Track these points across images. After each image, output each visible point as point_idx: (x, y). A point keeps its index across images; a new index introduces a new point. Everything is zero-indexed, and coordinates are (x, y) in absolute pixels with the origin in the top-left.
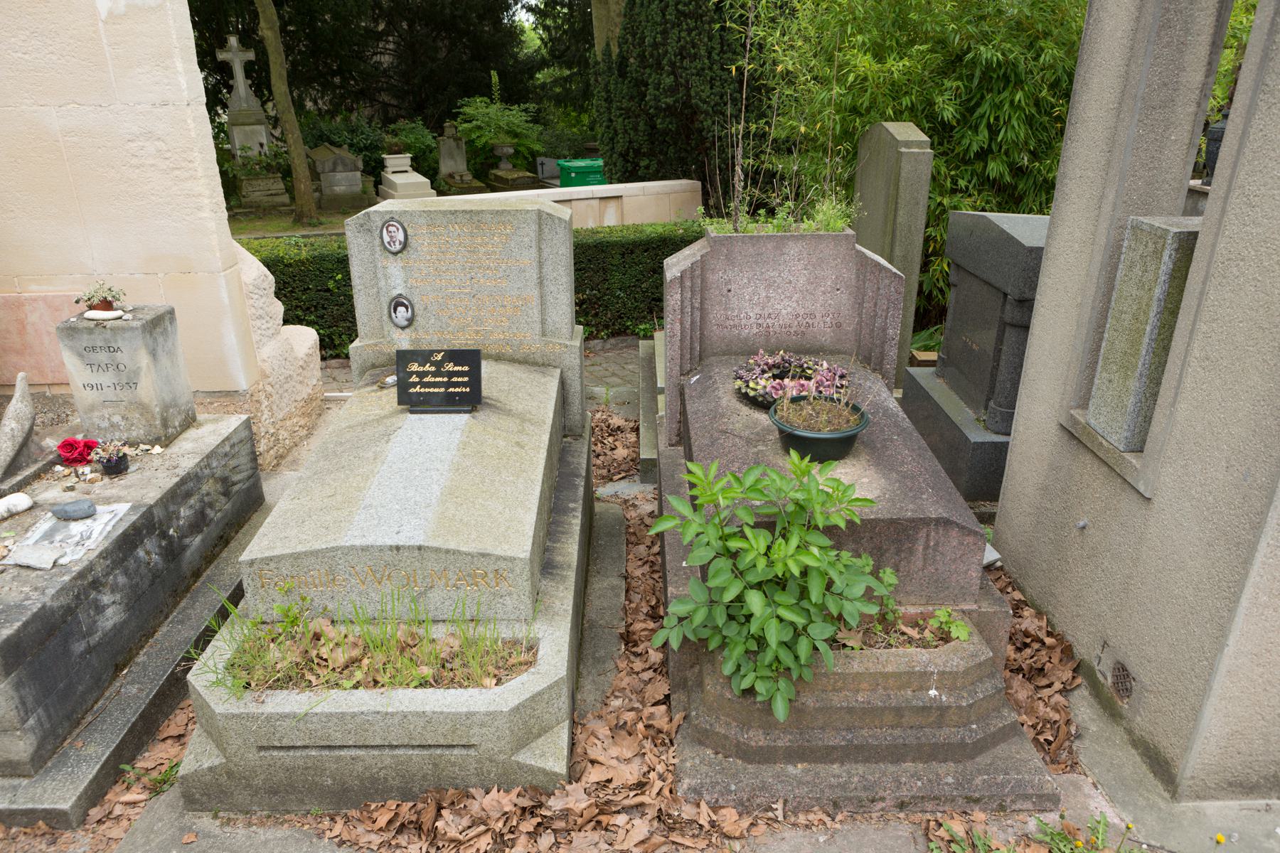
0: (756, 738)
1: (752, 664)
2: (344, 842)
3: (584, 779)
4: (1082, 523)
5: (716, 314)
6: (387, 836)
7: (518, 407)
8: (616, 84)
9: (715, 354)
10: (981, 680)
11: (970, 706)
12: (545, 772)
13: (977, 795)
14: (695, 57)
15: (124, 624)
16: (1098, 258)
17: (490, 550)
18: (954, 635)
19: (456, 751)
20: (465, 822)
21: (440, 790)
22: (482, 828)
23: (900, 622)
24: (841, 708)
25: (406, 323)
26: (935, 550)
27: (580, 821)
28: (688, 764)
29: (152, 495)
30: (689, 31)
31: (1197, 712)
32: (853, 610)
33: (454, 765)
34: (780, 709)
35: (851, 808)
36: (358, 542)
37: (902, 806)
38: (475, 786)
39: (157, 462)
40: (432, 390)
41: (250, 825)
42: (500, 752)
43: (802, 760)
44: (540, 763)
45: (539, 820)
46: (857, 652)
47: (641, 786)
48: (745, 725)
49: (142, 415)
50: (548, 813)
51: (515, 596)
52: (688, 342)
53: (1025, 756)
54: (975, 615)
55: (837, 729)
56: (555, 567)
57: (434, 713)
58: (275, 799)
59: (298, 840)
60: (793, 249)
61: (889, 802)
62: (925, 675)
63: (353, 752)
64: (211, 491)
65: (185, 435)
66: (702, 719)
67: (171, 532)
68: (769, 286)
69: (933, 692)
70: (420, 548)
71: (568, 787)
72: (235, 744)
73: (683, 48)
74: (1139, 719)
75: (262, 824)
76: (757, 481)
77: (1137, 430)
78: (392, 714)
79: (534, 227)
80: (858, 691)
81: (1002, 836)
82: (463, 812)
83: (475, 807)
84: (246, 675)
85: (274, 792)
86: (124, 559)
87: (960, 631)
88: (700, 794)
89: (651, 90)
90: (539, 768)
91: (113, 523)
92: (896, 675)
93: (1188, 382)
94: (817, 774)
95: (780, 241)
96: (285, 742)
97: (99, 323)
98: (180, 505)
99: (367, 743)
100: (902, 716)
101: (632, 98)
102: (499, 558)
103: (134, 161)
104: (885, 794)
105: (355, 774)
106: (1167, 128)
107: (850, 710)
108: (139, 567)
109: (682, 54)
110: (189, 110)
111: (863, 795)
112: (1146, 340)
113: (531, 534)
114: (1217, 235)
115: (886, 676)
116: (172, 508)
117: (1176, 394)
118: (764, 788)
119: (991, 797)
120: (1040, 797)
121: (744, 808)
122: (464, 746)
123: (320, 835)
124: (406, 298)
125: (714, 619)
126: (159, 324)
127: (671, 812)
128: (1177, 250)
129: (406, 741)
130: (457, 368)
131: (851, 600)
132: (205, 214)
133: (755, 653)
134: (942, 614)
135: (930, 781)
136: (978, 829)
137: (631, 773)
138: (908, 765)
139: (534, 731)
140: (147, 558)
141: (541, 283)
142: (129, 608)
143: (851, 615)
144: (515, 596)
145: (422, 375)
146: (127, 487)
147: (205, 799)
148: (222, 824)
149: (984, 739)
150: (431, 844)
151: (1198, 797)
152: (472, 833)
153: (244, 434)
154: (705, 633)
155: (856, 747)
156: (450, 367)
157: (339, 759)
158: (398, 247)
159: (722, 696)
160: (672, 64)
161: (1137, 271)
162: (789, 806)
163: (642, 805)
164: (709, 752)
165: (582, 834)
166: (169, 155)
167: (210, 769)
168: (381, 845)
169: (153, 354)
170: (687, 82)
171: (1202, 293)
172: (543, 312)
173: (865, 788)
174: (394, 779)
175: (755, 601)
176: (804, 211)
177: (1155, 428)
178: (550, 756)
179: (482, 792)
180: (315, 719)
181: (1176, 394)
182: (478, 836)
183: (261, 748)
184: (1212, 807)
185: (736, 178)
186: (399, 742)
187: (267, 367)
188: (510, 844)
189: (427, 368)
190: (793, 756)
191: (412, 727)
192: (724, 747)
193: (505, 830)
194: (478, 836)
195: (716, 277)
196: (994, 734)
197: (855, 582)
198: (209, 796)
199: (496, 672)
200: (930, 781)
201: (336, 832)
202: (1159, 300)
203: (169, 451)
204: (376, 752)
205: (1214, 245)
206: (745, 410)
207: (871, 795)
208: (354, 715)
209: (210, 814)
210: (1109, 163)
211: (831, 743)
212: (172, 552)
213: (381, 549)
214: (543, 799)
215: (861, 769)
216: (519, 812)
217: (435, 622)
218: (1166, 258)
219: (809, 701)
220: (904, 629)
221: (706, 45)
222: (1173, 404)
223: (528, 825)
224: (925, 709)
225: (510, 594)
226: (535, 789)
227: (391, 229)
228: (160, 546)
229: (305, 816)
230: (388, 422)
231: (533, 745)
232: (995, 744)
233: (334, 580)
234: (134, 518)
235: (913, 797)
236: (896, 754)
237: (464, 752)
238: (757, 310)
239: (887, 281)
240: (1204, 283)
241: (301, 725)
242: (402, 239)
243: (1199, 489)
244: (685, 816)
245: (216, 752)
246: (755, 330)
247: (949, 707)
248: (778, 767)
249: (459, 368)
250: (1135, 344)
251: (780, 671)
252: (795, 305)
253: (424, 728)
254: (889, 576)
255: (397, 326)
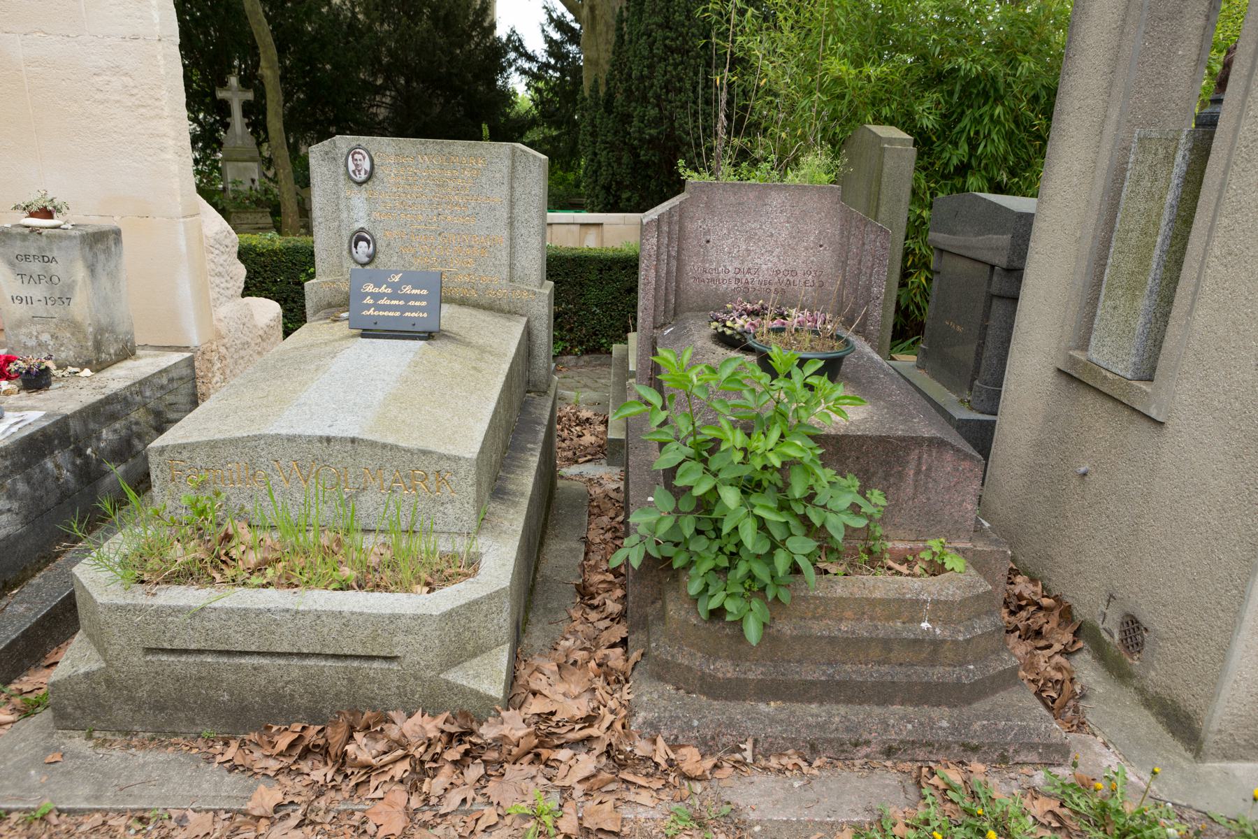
0: (724, 669)
1: (721, 583)
2: (236, 767)
3: (524, 710)
4: (1082, 470)
5: (693, 266)
6: (287, 761)
7: (475, 340)
8: (602, 118)
9: (690, 310)
10: (978, 616)
11: (968, 641)
12: (477, 695)
13: (975, 742)
14: (680, 90)
15: (19, 538)
16: (1100, 183)
17: (432, 448)
18: (948, 566)
19: (376, 664)
20: (381, 746)
21: (355, 712)
22: (400, 752)
23: (887, 556)
24: (822, 637)
25: (367, 259)
26: (927, 476)
27: (515, 751)
28: (645, 699)
29: (70, 407)
30: (676, 66)
31: (1224, 651)
32: (836, 525)
33: (372, 681)
34: (752, 632)
35: (831, 753)
36: (284, 432)
37: (889, 752)
38: (395, 709)
39: (82, 383)
40: (386, 313)
41: (128, 746)
42: (427, 667)
43: (776, 696)
44: (473, 684)
45: (468, 746)
46: (840, 578)
47: (589, 720)
48: (712, 655)
49: (73, 334)
50: (479, 741)
51: (458, 504)
52: (662, 292)
53: (1026, 704)
54: (970, 554)
55: (815, 663)
56: (505, 493)
57: (352, 613)
58: (162, 717)
59: (182, 764)
60: (776, 199)
61: (874, 748)
62: (917, 603)
63: (256, 661)
64: (142, 421)
65: (119, 365)
66: (662, 648)
67: (89, 451)
68: (750, 238)
69: (925, 625)
70: (353, 440)
71: (504, 714)
72: (118, 643)
73: (669, 82)
74: (1153, 673)
75: (143, 746)
76: (733, 374)
77: (1146, 355)
78: (304, 613)
79: (508, 162)
80: (841, 620)
81: (1005, 788)
82: (379, 736)
83: (394, 732)
84: (141, 571)
85: (159, 707)
86: (28, 465)
87: (954, 562)
88: (657, 730)
89: (636, 122)
90: (472, 690)
91: (20, 425)
92: (885, 602)
93: (1207, 285)
94: (793, 713)
95: (764, 190)
96: (177, 644)
97: (33, 230)
98: (102, 425)
99: (272, 649)
100: (891, 650)
101: (615, 133)
102: (442, 457)
103: (99, 96)
104: (870, 737)
105: (256, 688)
106: (1174, 42)
107: (832, 640)
108: (45, 479)
109: (667, 87)
110: (160, 46)
111: (845, 736)
112: (1157, 252)
113: (481, 439)
114: (1239, 117)
115: (872, 602)
116: (92, 426)
117: (1193, 301)
118: (731, 724)
119: (991, 745)
120: (1047, 746)
121: (707, 747)
122: (385, 658)
123: (209, 760)
124: (367, 233)
125: (681, 530)
126: (101, 242)
127: (621, 747)
128: (1191, 150)
129: (318, 649)
130: (415, 292)
131: (836, 513)
132: (169, 156)
133: (727, 570)
134: (935, 544)
135: (921, 724)
136: (977, 778)
137: (581, 708)
138: (897, 708)
139: (469, 647)
140: (56, 472)
141: (511, 224)
142: (27, 521)
143: (837, 528)
144: (458, 504)
145: (376, 296)
146: (44, 400)
147: (78, 713)
148: (96, 746)
149: (982, 681)
150: (338, 771)
151: (1227, 757)
152: (387, 758)
153: (185, 372)
154: (669, 550)
155: (838, 683)
156: (408, 290)
157: (239, 668)
158: (363, 176)
159: (686, 621)
160: (658, 97)
161: (1146, 183)
162: (760, 748)
163: (589, 739)
164: (669, 687)
165: (518, 766)
166: (135, 91)
167: (87, 675)
168: (278, 772)
169: (92, 269)
170: (671, 114)
171: (1222, 185)
172: (512, 255)
173: (848, 730)
174: (301, 697)
175: (730, 497)
176: (786, 162)
177: (1168, 344)
178: (486, 676)
179: (404, 715)
180: (213, 616)
181: (1193, 301)
182: (394, 762)
183: (149, 651)
184: (1240, 768)
185: (719, 125)
186: (311, 650)
187: (223, 328)
188: (431, 773)
189: (383, 289)
190: (768, 691)
191: (326, 630)
192: (686, 681)
193: (427, 757)
194: (394, 762)
195: (694, 226)
196: (993, 677)
197: (841, 501)
198: (83, 709)
199: (430, 580)
200: (921, 724)
201: (228, 756)
202: (1172, 206)
203: (98, 376)
204: (282, 662)
205: (1236, 130)
206: (721, 350)
207: (853, 737)
208: (259, 613)
209: (83, 734)
210: (1111, 84)
211: (809, 678)
212: (89, 475)
213: (310, 440)
214: (475, 726)
215: (843, 709)
216: (444, 739)
217: (366, 531)
218: (1179, 159)
219: (786, 628)
220: (891, 563)
221: (691, 79)
222: (1190, 313)
223: (455, 753)
224: (916, 642)
225: (452, 501)
226: (465, 715)
227: (357, 156)
228: (74, 463)
229: (195, 739)
230: (336, 344)
231: (467, 664)
232: (994, 691)
233: (254, 475)
234: (45, 424)
235: (902, 742)
236: (882, 694)
237: (385, 665)
238: (737, 264)
239: (872, 236)
240: (1225, 173)
241: (197, 623)
242: (368, 168)
243: (1223, 398)
244: (638, 752)
245: (97, 656)
246: (733, 286)
247: (943, 641)
248: (748, 705)
249: (418, 292)
250: (1143, 261)
251: (754, 588)
252: (776, 260)
253: (340, 632)
254: (877, 496)
255: (356, 262)
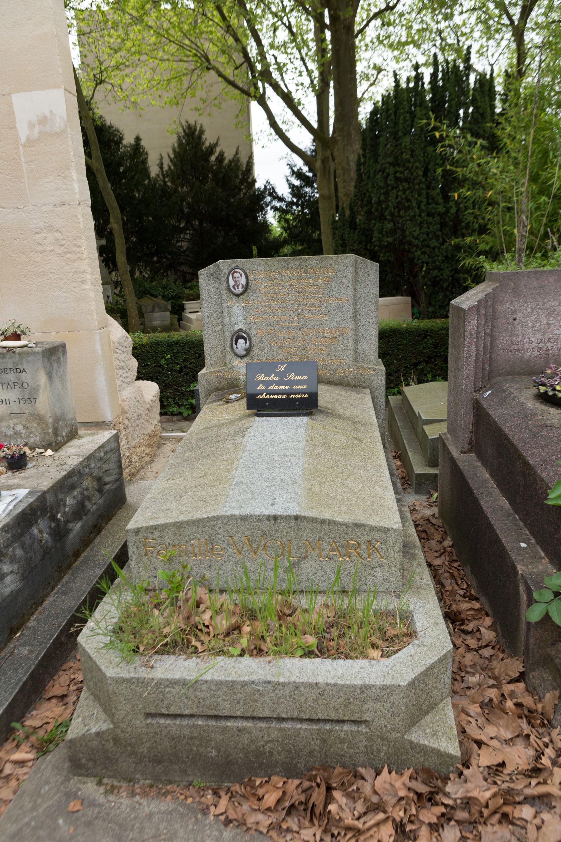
2: (231, 821)
5: (503, 340)
6: (273, 818)
8: (349, 234)
9: (500, 375)
14: (409, 208)
17: (363, 521)
19: (346, 727)
21: (326, 767)
25: (244, 353)
29: (45, 484)
30: (404, 191)
33: (343, 741)
36: (237, 512)
39: (49, 461)
41: (133, 794)
42: (393, 730)
44: (432, 743)
49: (38, 424)
50: (450, 802)
51: (386, 568)
52: (480, 363)
57: (327, 684)
58: (159, 769)
64: (90, 486)
65: (69, 444)
67: (59, 516)
68: (550, 314)
70: (296, 518)
73: (400, 203)
75: (145, 794)
78: (284, 685)
79: (352, 270)
86: (22, 535)
89: (376, 234)
90: (433, 749)
91: (14, 503)
96: (173, 710)
97: (10, 350)
98: (66, 494)
99: (255, 715)
101: (360, 243)
102: (373, 529)
103: (39, 248)
105: (240, 746)
108: (33, 542)
109: (399, 206)
110: (79, 208)
116: (60, 496)
122: (354, 722)
126: (54, 353)
129: (295, 714)
132: (88, 286)
139: (424, 707)
140: (40, 536)
141: (355, 318)
144: (386, 568)
146: (25, 478)
147: (90, 764)
150: (325, 831)
153: (114, 445)
156: (291, 377)
157: (225, 730)
158: (241, 290)
160: (392, 215)
166: (64, 242)
167: (98, 734)
168: (271, 827)
169: (50, 375)
170: (403, 225)
172: (356, 342)
174: (279, 754)
178: (439, 735)
179: (372, 772)
183: (149, 715)
186: (289, 715)
187: (126, 406)
189: (272, 377)
191: (303, 699)
195: (504, 307)
198: (95, 761)
201: (222, 808)
203: (58, 454)
204: (263, 725)
208: (244, 684)
209: (96, 780)
212: (59, 533)
213: (259, 519)
221: (416, 199)
223: (430, 815)
225: (381, 566)
227: (235, 275)
228: (50, 527)
230: (240, 423)
231: (422, 722)
233: (212, 549)
234: (31, 500)
237: (354, 728)
238: (539, 336)
242: (244, 283)
245: (103, 716)
246: (536, 353)
253: (315, 700)
255: (237, 355)
